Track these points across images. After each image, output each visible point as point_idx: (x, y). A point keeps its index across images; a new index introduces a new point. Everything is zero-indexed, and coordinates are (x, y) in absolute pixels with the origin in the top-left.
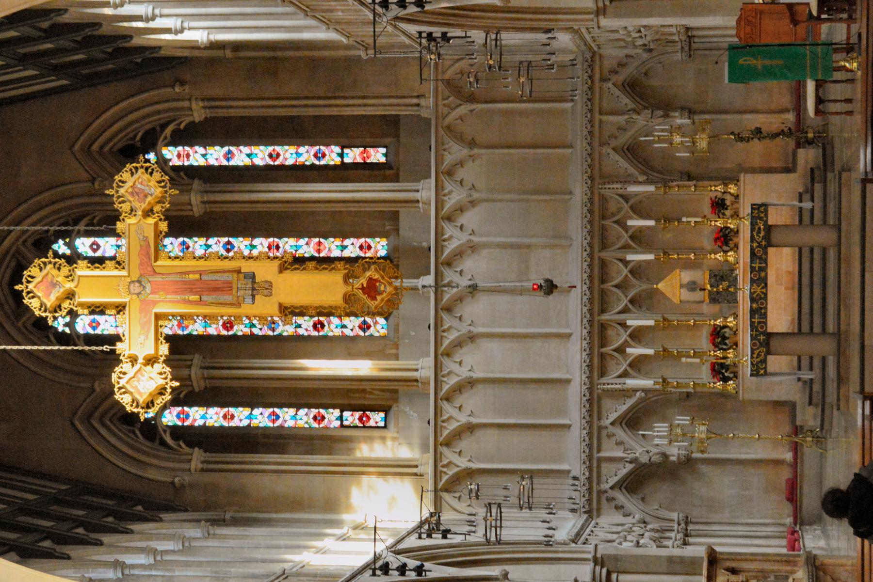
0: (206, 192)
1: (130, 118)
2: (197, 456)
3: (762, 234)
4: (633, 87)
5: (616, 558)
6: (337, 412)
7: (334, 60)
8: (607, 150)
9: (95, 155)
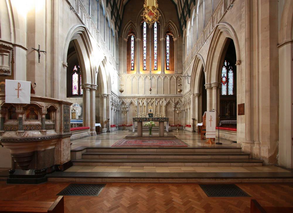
0: (163, 41)
1: (174, 29)
2: (126, 40)
3: (162, 120)
4: (178, 102)
5: (109, 98)
6: (133, 63)
7: (182, 59)
8: (169, 99)
9: (169, 24)
